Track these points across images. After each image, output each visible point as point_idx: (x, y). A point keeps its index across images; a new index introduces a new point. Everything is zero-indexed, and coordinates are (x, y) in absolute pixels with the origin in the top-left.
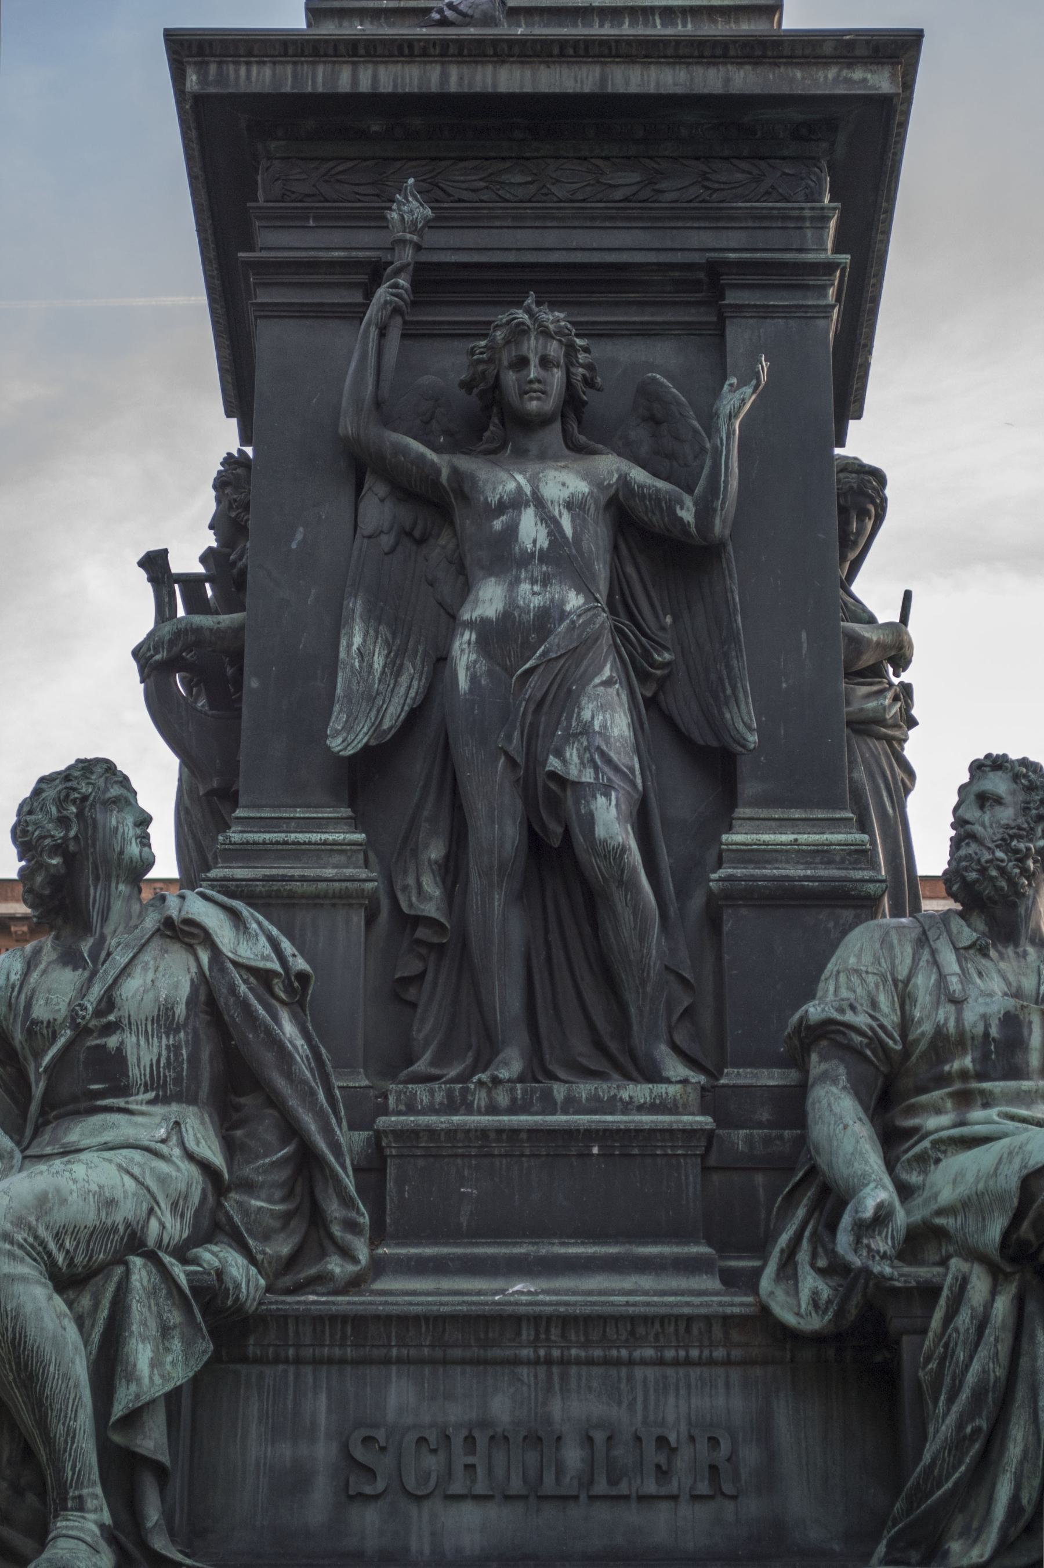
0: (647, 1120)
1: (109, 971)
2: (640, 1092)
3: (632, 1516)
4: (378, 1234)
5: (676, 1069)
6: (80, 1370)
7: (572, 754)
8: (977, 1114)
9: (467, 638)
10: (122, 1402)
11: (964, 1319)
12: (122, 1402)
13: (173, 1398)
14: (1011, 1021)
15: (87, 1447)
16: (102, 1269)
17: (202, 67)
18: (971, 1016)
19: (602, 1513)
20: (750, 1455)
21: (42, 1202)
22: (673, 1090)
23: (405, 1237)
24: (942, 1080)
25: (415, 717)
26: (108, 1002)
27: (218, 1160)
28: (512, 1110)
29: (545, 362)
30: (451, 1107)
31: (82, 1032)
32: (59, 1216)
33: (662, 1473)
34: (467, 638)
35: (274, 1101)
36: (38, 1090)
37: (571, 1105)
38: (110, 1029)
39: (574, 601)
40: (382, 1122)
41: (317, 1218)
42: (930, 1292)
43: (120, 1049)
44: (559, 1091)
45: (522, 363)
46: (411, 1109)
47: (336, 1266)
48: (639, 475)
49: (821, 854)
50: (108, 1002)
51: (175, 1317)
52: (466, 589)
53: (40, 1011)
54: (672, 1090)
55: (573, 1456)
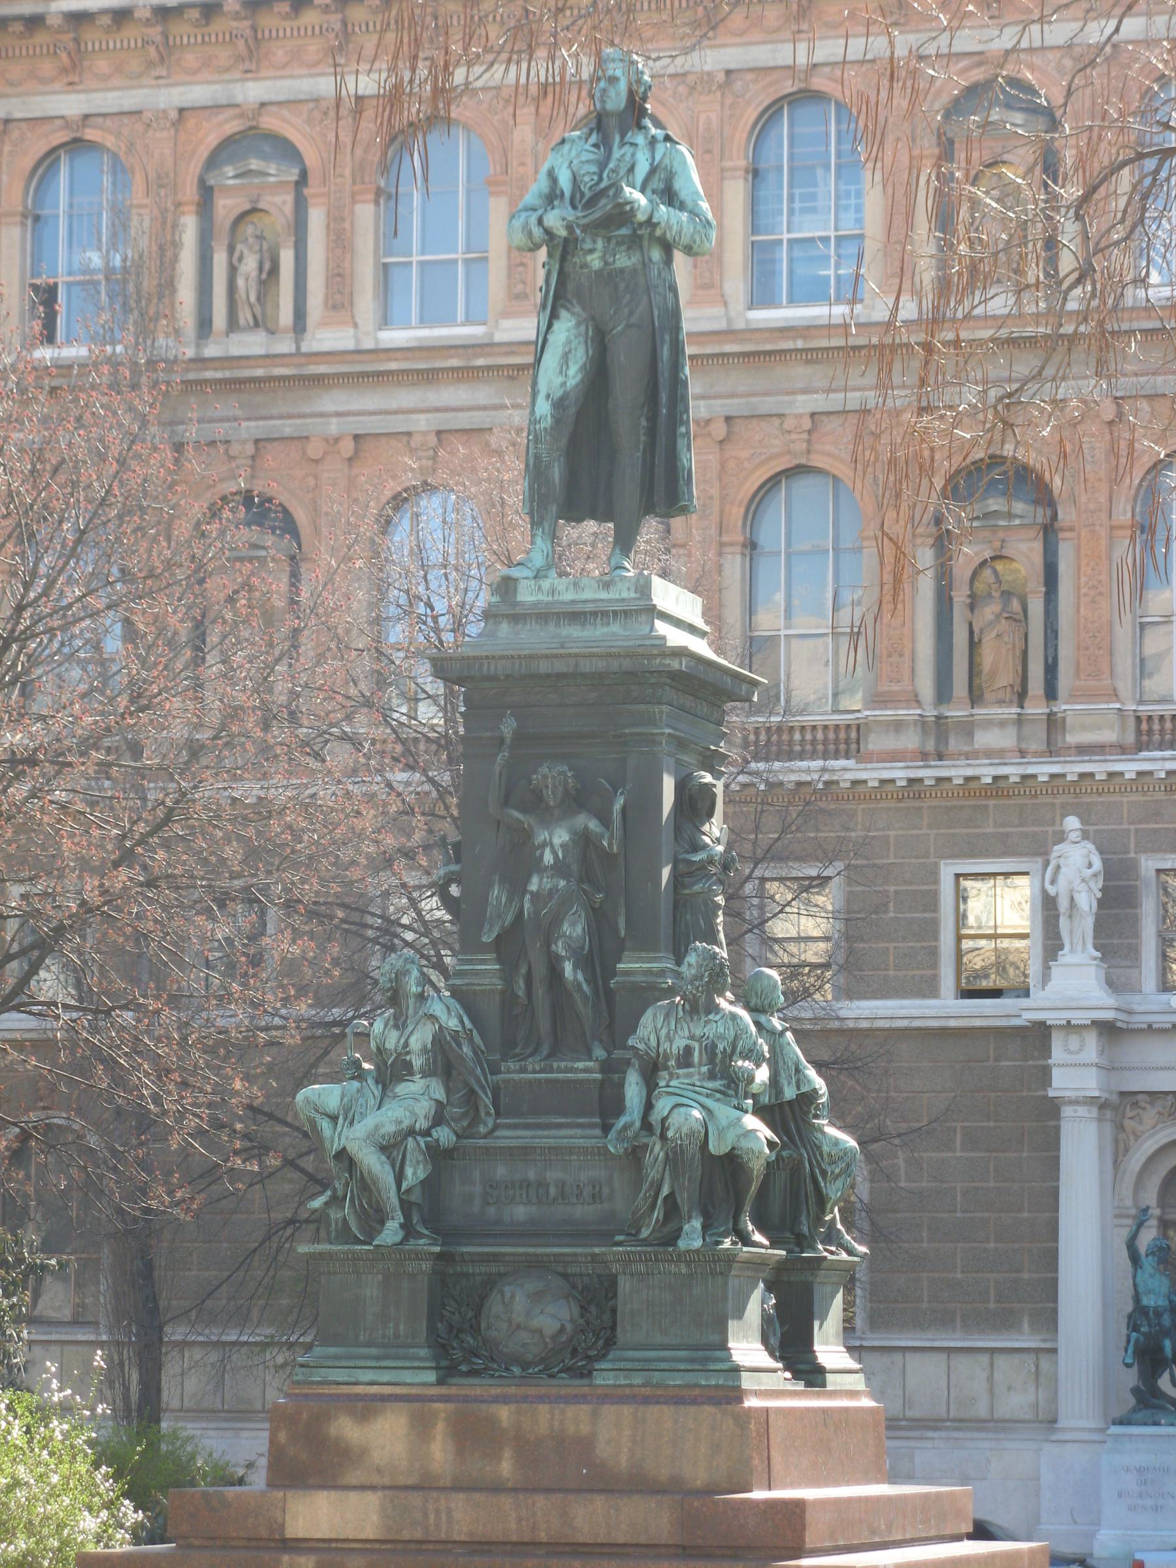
1: (407, 1032)
4: (498, 1114)
5: (599, 1053)
6: (391, 1179)
7: (560, 944)
9: (528, 896)
12: (404, 1186)
14: (688, 1050)
15: (395, 1201)
16: (402, 1141)
18: (674, 1047)
21: (377, 1128)
22: (591, 1064)
28: (541, 1072)
30: (523, 1070)
31: (399, 1055)
32: (383, 1131)
37: (559, 1071)
38: (408, 1053)
39: (562, 883)
43: (410, 1062)
44: (555, 1065)
46: (509, 1072)
48: (594, 825)
49: (649, 972)
50: (406, 1044)
51: (421, 1158)
52: (528, 879)
55: (553, 1191)
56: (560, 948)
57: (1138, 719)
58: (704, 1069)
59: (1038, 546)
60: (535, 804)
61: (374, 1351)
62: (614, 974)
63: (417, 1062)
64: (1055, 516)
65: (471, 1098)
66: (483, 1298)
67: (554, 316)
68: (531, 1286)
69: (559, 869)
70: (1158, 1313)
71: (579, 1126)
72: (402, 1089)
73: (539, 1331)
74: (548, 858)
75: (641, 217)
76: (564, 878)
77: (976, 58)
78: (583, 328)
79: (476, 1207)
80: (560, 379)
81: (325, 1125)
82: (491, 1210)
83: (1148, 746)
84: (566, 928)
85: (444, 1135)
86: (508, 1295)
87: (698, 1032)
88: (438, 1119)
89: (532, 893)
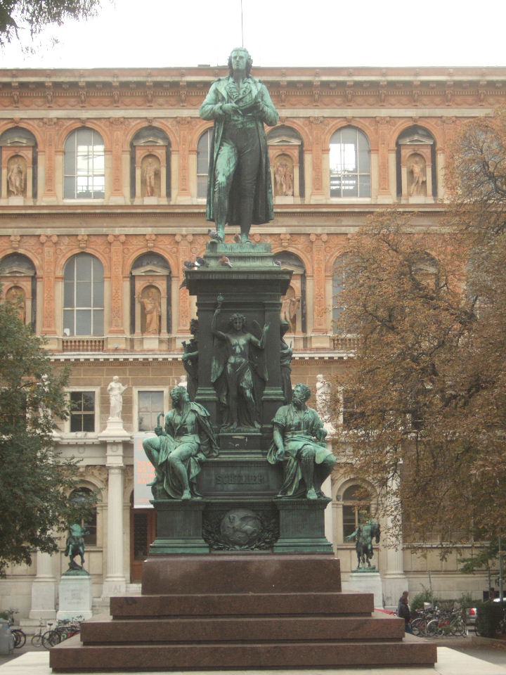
0: (253, 434)
2: (252, 430)
3: (252, 486)
5: (258, 426)
6: (185, 473)
7: (244, 383)
8: (295, 436)
9: (229, 365)
10: (191, 476)
11: (291, 465)
12: (191, 476)
13: (197, 476)
14: (299, 423)
15: (187, 482)
17: (190, 275)
19: (248, 485)
20: (265, 478)
23: (224, 449)
24: (290, 431)
25: (222, 373)
26: (185, 422)
27: (199, 442)
29: (240, 323)
33: (255, 480)
34: (229, 365)
35: (206, 433)
36: (176, 432)
39: (244, 360)
40: (220, 434)
41: (211, 447)
42: (287, 461)
45: (236, 323)
47: (215, 454)
48: (253, 338)
49: (276, 394)
50: (185, 422)
53: (176, 422)
54: (256, 430)
55: (244, 478)
56: (244, 385)
57: (63, 342)
58: (305, 431)
59: (30, 283)
60: (234, 330)
61: (181, 541)
62: (263, 395)
63: (189, 428)
64: (36, 273)
65: (210, 442)
66: (221, 520)
67: (221, 145)
68: (242, 513)
69: (242, 354)
70: (78, 539)
71: (253, 453)
72: (184, 438)
73: (245, 532)
74: (238, 350)
75: (261, 109)
76: (244, 358)
77: (10, 121)
78: (233, 149)
79: (213, 484)
80: (228, 168)
81: (155, 453)
82: (219, 486)
83: (67, 350)
84: (246, 377)
85: (201, 456)
86: (232, 518)
87: (302, 417)
88: (199, 451)
89: (231, 363)
